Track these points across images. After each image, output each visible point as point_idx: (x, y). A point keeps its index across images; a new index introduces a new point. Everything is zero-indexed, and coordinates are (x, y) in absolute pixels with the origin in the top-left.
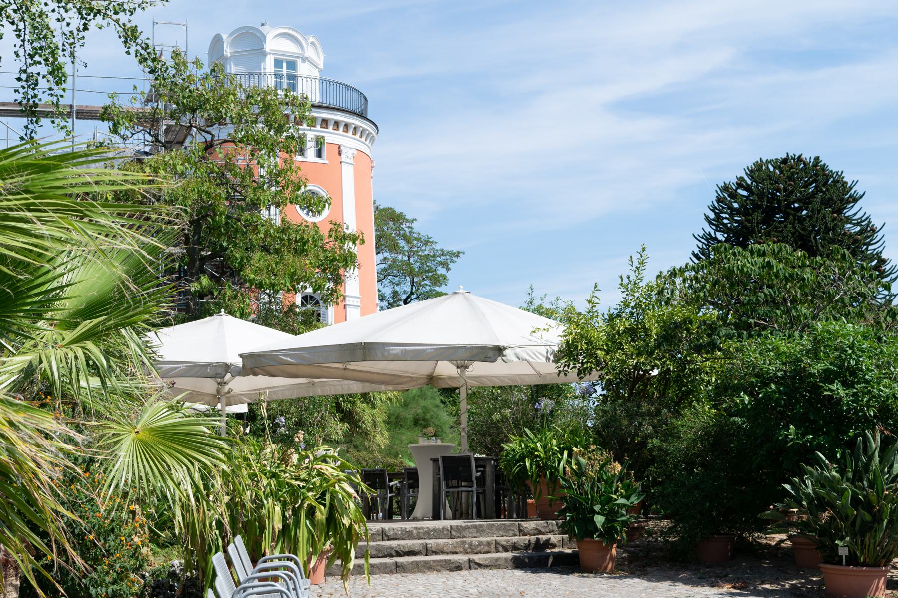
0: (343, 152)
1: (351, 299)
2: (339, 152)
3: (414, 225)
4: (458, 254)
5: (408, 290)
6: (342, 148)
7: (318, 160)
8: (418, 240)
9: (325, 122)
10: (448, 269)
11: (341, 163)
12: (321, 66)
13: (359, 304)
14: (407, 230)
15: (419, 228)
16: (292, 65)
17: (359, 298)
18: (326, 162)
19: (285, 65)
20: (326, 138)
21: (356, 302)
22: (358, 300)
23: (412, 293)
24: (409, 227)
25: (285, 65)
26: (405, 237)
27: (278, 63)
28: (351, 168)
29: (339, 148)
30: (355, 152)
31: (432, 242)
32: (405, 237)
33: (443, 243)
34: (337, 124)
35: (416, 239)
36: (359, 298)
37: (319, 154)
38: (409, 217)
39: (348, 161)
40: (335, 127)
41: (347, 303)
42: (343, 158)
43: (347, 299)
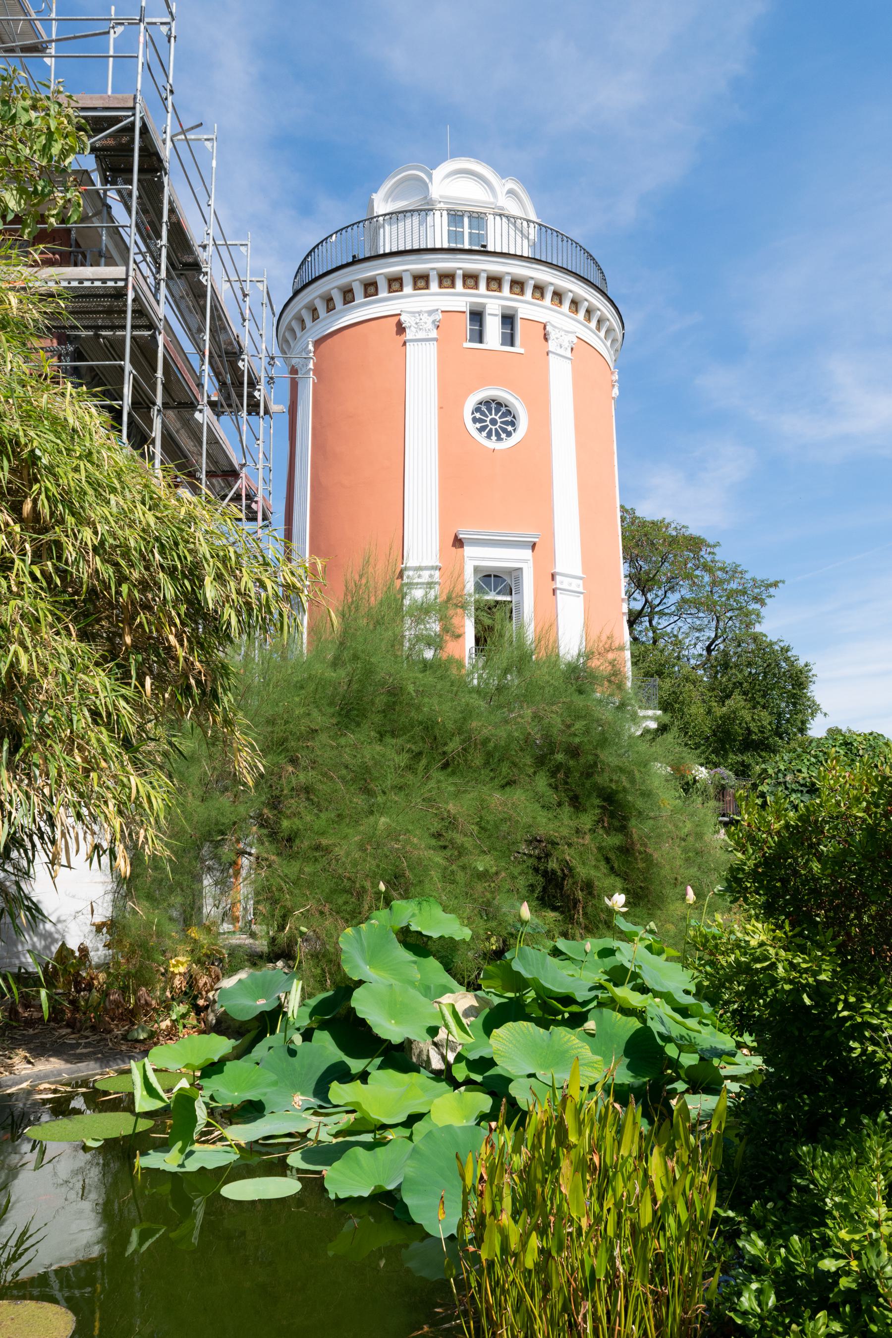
0: (552, 336)
1: (567, 580)
2: (545, 335)
3: (716, 550)
4: (775, 584)
5: (713, 635)
6: (548, 328)
8: (722, 569)
9: (518, 285)
10: (763, 604)
11: (548, 354)
13: (581, 589)
14: (709, 558)
15: (724, 556)
17: (581, 578)
18: (522, 351)
19: (466, 220)
20: (520, 311)
21: (577, 585)
22: (580, 582)
23: (716, 637)
24: (710, 553)
25: (466, 220)
26: (706, 568)
28: (567, 366)
29: (545, 328)
30: (575, 340)
31: (741, 573)
32: (706, 568)
33: (756, 571)
34: (539, 289)
35: (720, 569)
36: (581, 578)
37: (509, 339)
38: (711, 541)
40: (538, 295)
41: (558, 585)
42: (552, 345)
43: (558, 578)
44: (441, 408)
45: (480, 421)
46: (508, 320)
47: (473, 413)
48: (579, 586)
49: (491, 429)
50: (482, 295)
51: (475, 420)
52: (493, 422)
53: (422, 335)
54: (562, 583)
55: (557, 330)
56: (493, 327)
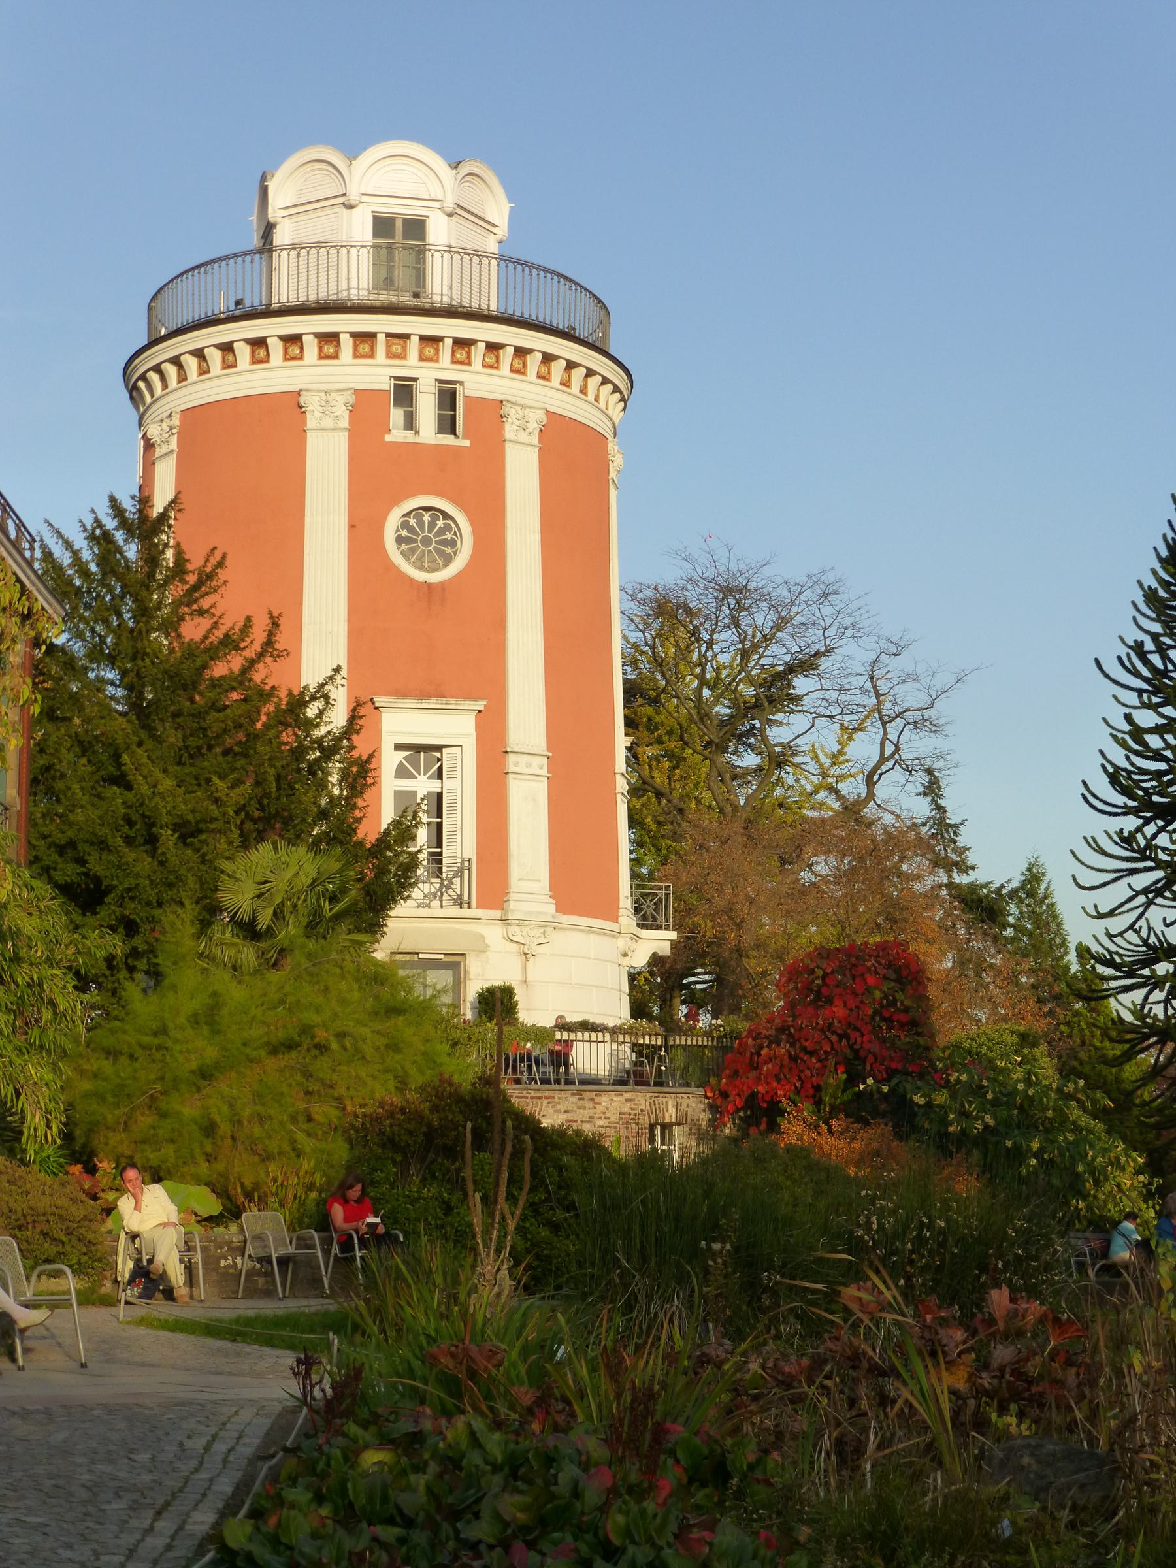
6: (507, 409)
7: (448, 440)
12: (502, 231)
16: (416, 227)
18: (467, 443)
27: (383, 225)
37: (448, 425)
39: (523, 437)
44: (352, 526)
45: (408, 540)
46: (448, 396)
47: (398, 530)
48: (541, 767)
49: (430, 532)
50: (411, 366)
51: (400, 540)
52: (426, 541)
53: (328, 422)
54: (516, 764)
55: (518, 408)
56: (427, 407)
